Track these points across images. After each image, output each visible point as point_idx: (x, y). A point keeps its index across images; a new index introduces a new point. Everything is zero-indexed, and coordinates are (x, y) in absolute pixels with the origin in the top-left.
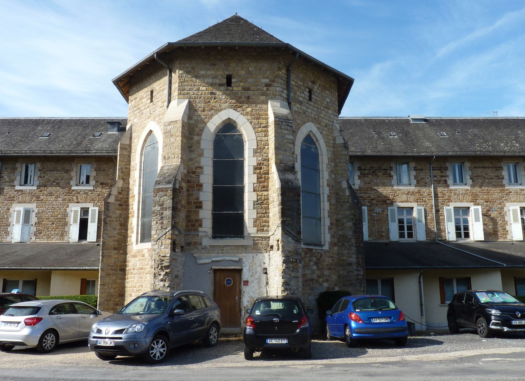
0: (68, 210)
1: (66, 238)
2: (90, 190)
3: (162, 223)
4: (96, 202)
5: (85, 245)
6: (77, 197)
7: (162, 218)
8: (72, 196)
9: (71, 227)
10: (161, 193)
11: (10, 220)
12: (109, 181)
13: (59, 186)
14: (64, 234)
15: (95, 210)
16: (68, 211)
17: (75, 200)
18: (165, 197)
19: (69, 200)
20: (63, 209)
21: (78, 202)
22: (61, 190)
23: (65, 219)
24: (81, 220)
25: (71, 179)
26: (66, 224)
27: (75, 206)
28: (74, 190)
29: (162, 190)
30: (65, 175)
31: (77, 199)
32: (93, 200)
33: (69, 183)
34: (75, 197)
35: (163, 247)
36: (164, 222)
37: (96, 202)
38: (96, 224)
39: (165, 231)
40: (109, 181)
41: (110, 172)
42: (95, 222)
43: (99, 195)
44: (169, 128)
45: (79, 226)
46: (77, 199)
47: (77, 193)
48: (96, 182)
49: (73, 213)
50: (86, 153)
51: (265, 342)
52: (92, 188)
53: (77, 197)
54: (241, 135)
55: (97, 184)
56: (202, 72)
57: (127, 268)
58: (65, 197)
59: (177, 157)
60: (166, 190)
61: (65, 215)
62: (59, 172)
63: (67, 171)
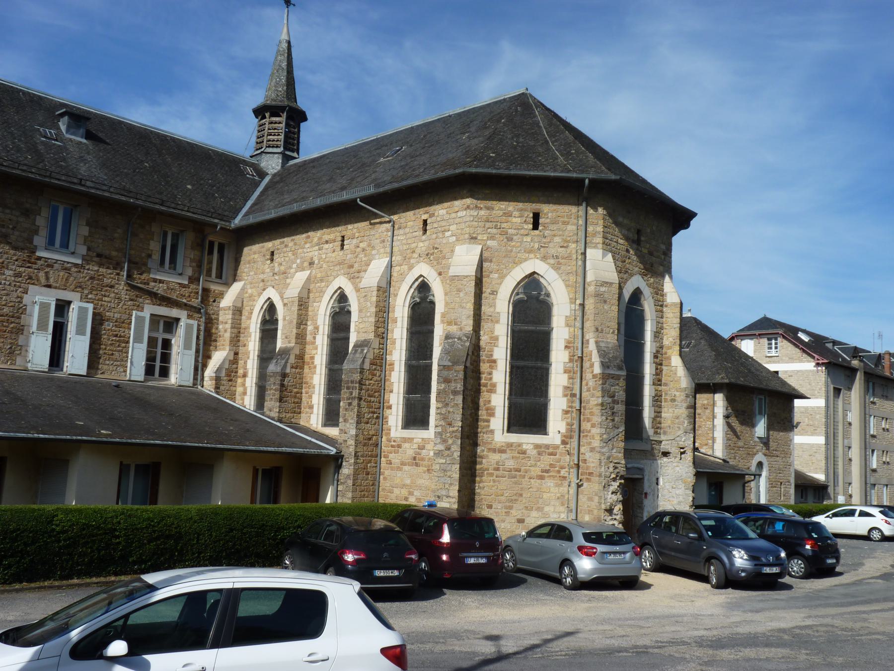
0: (26, 299)
1: (19, 361)
2: (76, 265)
3: (613, 420)
4: (86, 292)
5: (60, 379)
6: (47, 273)
7: (613, 413)
8: (34, 271)
9: (33, 337)
10: (612, 381)
11: (24, 319)
12: (114, 253)
13: (8, 243)
14: (16, 350)
15: (87, 309)
16: (25, 301)
17: (43, 280)
18: (617, 387)
19: (30, 278)
20: (15, 294)
21: (49, 286)
22: (12, 252)
23: (19, 318)
24: (56, 324)
25: (36, 232)
26: (20, 330)
27: (41, 294)
28: (40, 258)
29: (613, 377)
30: (21, 219)
31: (47, 278)
32: (79, 287)
33: (31, 241)
34: (42, 275)
35: (614, 451)
36: (616, 419)
37: (86, 292)
38: (86, 339)
39: (616, 431)
40: (114, 253)
41: (116, 235)
42: (46, 330)
43: (92, 278)
44: (603, 289)
45: (50, 337)
46: (47, 278)
47: (48, 266)
48: (89, 249)
49: (37, 308)
50: (80, 184)
51: (372, 574)
52: (79, 262)
53: (47, 273)
54: (643, 311)
55: (90, 253)
56: (620, 219)
57: (478, 467)
58: (22, 269)
59: (613, 333)
60: (618, 377)
61: (20, 311)
62: (8, 211)
63: (27, 213)
